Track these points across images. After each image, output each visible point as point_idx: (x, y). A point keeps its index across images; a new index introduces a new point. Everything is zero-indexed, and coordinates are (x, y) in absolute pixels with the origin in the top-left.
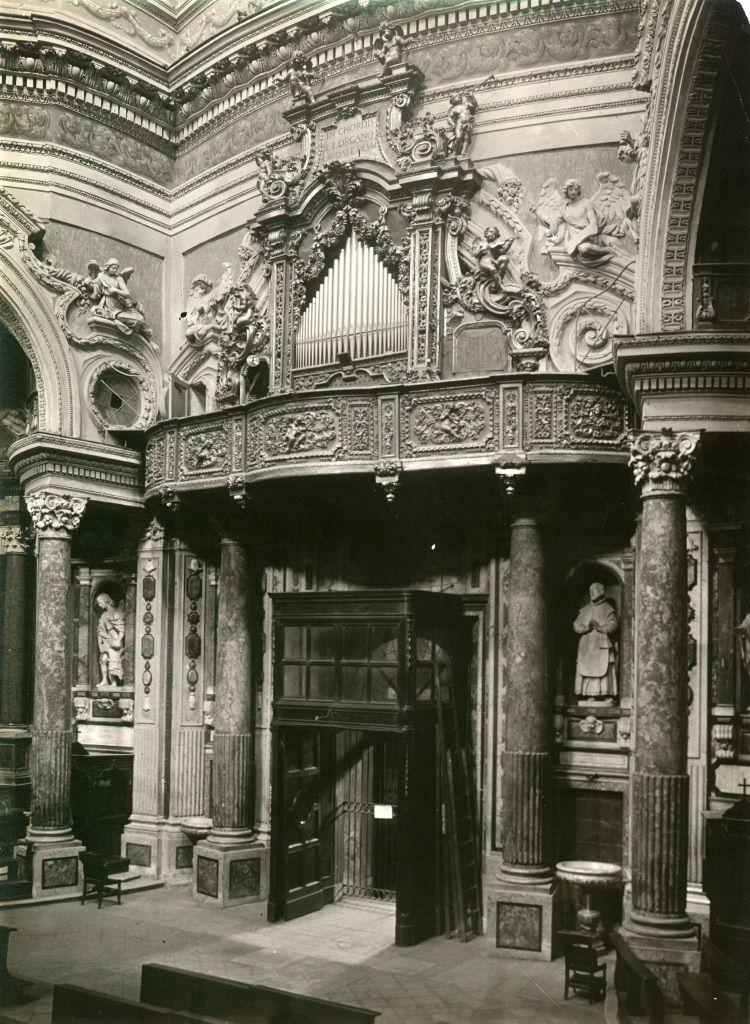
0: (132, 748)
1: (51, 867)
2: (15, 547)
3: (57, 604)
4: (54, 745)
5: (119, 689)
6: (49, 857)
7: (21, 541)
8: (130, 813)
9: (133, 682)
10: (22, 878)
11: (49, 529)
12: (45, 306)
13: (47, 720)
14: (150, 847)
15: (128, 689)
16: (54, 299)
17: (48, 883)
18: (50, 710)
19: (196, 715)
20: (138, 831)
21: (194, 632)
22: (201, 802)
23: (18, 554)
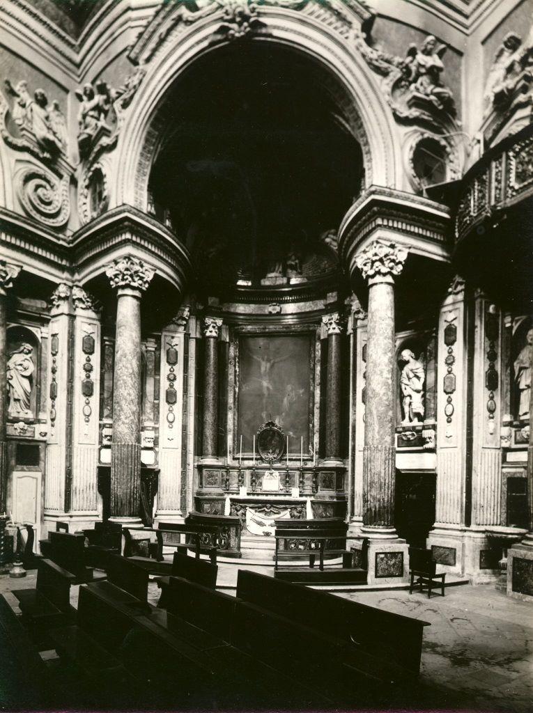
0: (433, 470)
1: (382, 559)
2: (334, 328)
3: (385, 338)
4: (383, 457)
5: (421, 424)
6: (381, 551)
7: (338, 324)
8: (434, 520)
9: (435, 416)
10: (355, 566)
11: (378, 276)
12: (375, 86)
13: (377, 436)
14: (455, 549)
15: (430, 421)
16: (381, 81)
17: (380, 573)
18: (380, 428)
19: (494, 439)
20: (442, 536)
21: (492, 367)
22: (499, 514)
23: (336, 334)
